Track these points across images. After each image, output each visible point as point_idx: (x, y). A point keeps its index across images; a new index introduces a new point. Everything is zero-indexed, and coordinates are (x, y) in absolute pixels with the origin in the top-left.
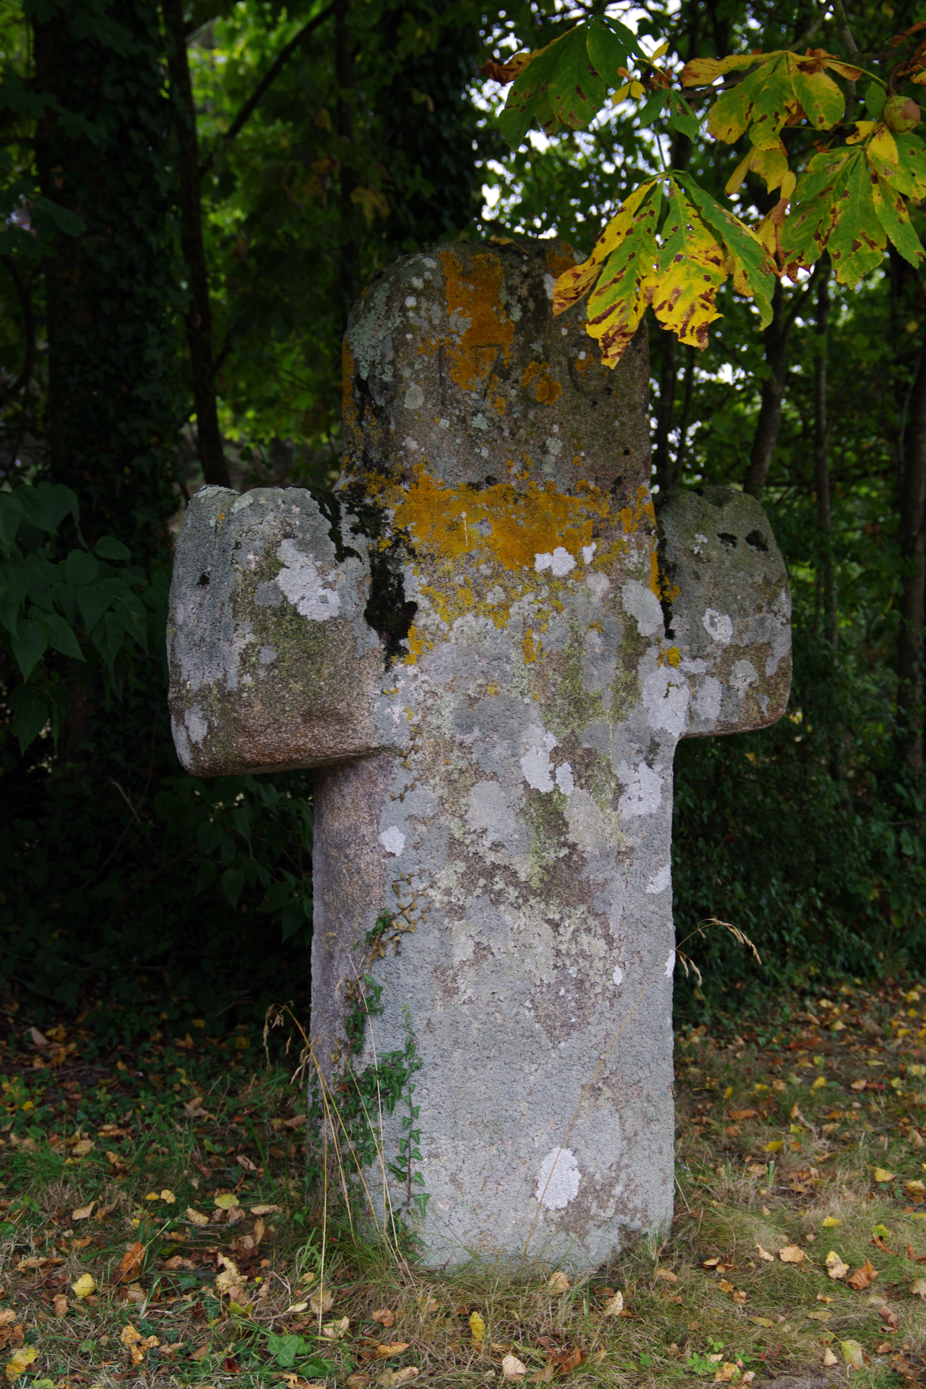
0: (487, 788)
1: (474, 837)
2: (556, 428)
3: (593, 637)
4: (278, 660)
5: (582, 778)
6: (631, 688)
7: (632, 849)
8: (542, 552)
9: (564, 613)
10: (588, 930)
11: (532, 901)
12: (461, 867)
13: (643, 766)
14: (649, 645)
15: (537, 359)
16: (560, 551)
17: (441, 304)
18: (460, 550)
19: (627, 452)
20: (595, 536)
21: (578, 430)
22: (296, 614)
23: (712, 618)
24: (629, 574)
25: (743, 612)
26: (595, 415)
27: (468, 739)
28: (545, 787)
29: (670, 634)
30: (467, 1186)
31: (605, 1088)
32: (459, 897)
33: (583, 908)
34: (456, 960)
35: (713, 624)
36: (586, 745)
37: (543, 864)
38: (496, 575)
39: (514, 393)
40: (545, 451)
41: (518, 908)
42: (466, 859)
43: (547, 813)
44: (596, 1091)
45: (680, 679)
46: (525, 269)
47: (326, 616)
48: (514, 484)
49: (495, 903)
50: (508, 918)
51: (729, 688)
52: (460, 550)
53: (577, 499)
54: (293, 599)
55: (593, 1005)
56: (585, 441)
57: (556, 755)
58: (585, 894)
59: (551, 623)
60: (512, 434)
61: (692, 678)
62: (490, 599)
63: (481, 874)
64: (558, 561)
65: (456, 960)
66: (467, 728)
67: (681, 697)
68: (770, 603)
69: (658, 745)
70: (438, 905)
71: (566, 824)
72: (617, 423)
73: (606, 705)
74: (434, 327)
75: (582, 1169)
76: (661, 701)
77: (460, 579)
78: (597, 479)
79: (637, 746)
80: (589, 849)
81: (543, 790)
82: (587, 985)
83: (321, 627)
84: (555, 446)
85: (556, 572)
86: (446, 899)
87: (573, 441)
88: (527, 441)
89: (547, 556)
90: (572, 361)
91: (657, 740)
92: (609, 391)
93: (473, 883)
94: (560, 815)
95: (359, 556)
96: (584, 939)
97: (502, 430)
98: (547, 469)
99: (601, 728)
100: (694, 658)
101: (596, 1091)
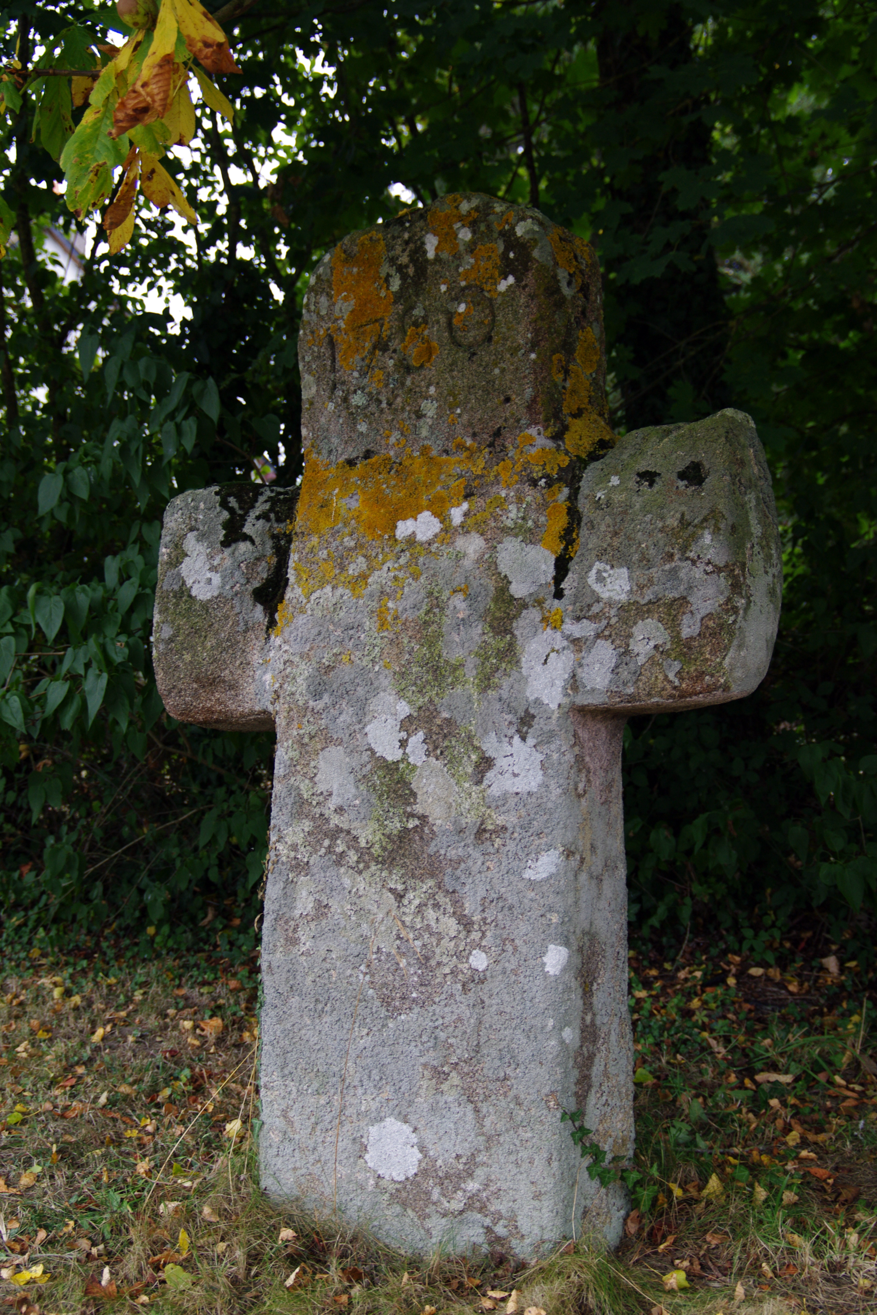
0: (335, 753)
1: (321, 798)
2: (432, 390)
3: (459, 603)
4: (175, 636)
5: (434, 748)
6: (509, 654)
7: (504, 828)
8: (405, 519)
9: (422, 580)
10: (436, 906)
11: (373, 868)
12: (307, 825)
13: (517, 739)
14: (525, 606)
15: (416, 324)
16: (426, 516)
17: (328, 294)
18: (325, 526)
19: (508, 400)
20: (468, 496)
21: (455, 386)
22: (190, 596)
23: (599, 572)
24: (506, 531)
25: (646, 562)
26: (474, 366)
27: (319, 705)
28: (392, 754)
29: (559, 594)
30: (297, 1125)
31: (454, 1074)
32: (303, 855)
33: (431, 883)
34: (297, 913)
35: (600, 579)
36: (445, 715)
37: (387, 831)
38: (359, 546)
39: (391, 363)
40: (419, 415)
41: (360, 873)
42: (313, 819)
43: (393, 783)
44: (439, 1075)
45: (560, 642)
46: (406, 236)
47: (208, 596)
48: (392, 453)
49: (338, 863)
50: (347, 882)
51: (627, 652)
52: (325, 526)
53: (454, 459)
54: (189, 582)
55: (441, 985)
56: (461, 397)
57: (408, 724)
58: (433, 869)
59: (406, 589)
60: (390, 404)
61: (576, 643)
62: (353, 570)
63: (326, 835)
64: (423, 526)
65: (297, 913)
66: (317, 695)
67: (560, 667)
68: (684, 549)
69: (533, 717)
70: (284, 859)
71: (414, 794)
72: (497, 371)
73: (470, 674)
74: (322, 318)
75: (422, 1149)
76: (539, 668)
77: (323, 554)
78: (474, 435)
79: (509, 717)
80: (438, 822)
81: (390, 758)
82: (433, 963)
83: (205, 606)
84: (430, 408)
85: (421, 537)
86: (292, 854)
87: (449, 400)
88: (403, 409)
89: (410, 523)
90: (450, 315)
91: (532, 711)
92: (489, 339)
93: (319, 842)
94: (407, 785)
95: (253, 542)
96: (431, 914)
97: (380, 402)
98: (424, 432)
99: (461, 698)
100: (578, 619)
101: (439, 1075)
